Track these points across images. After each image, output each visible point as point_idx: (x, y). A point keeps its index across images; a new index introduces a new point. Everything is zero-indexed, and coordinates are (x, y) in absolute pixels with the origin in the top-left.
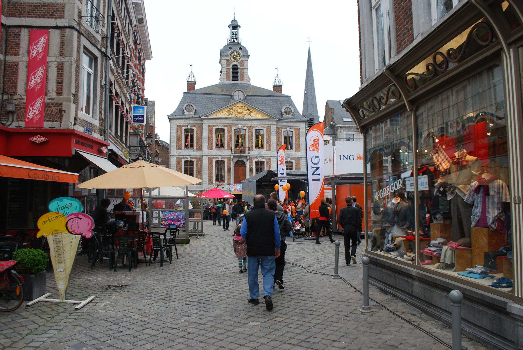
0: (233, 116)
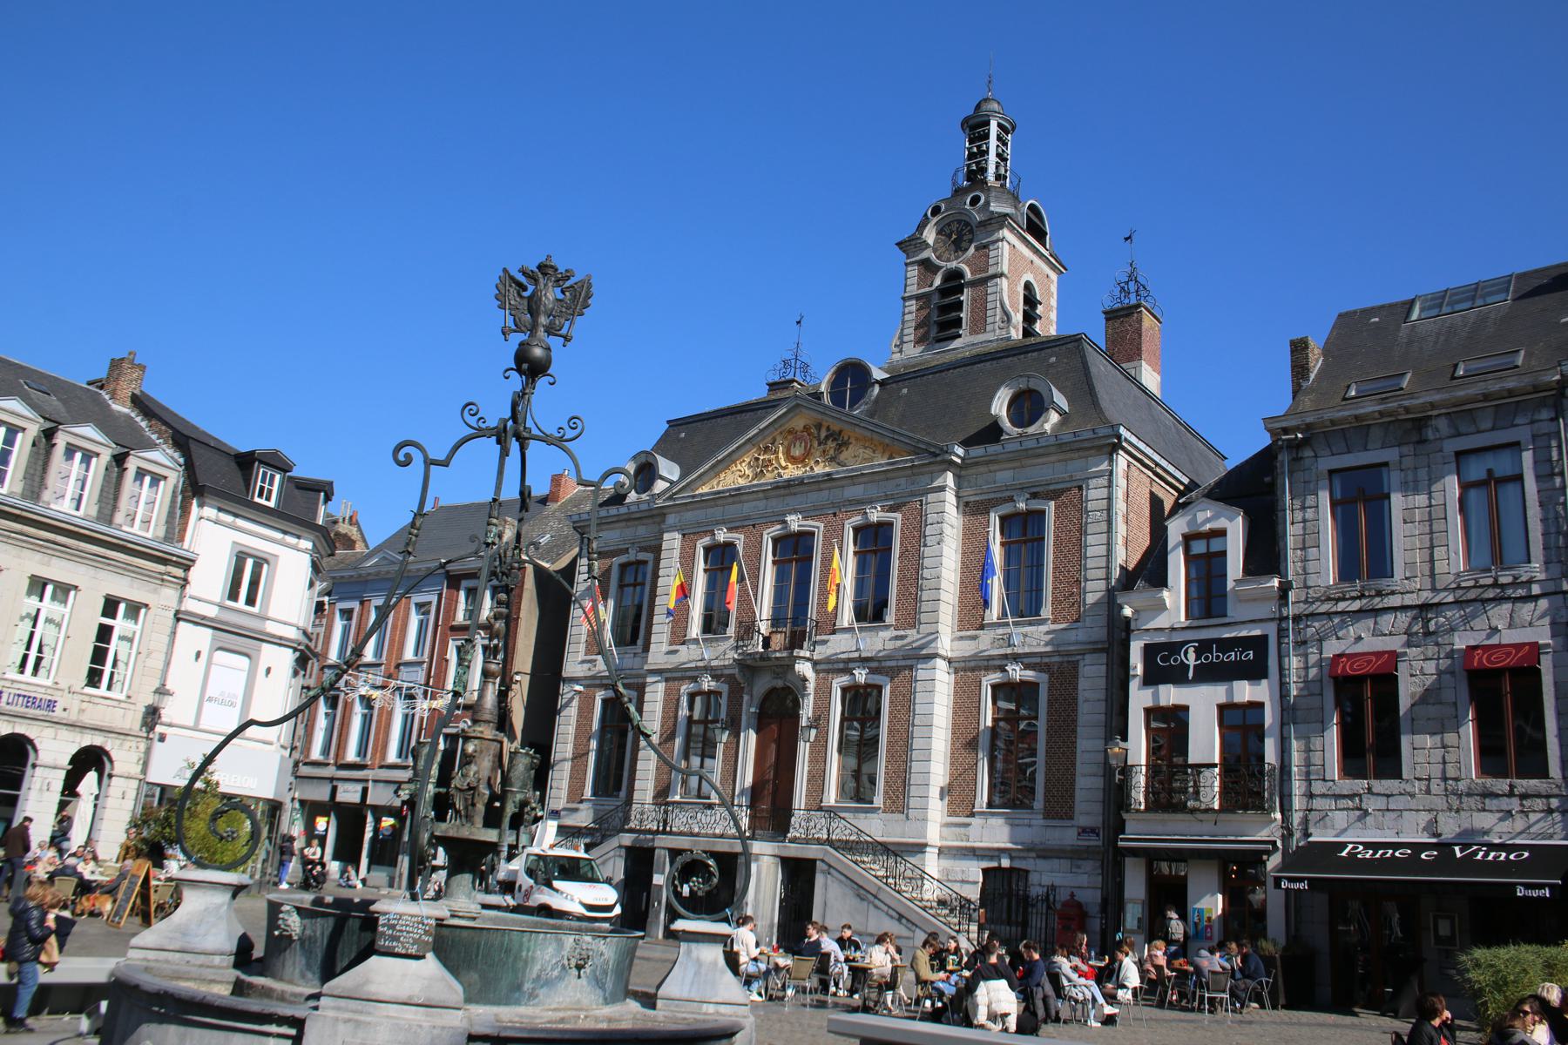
0: (769, 478)
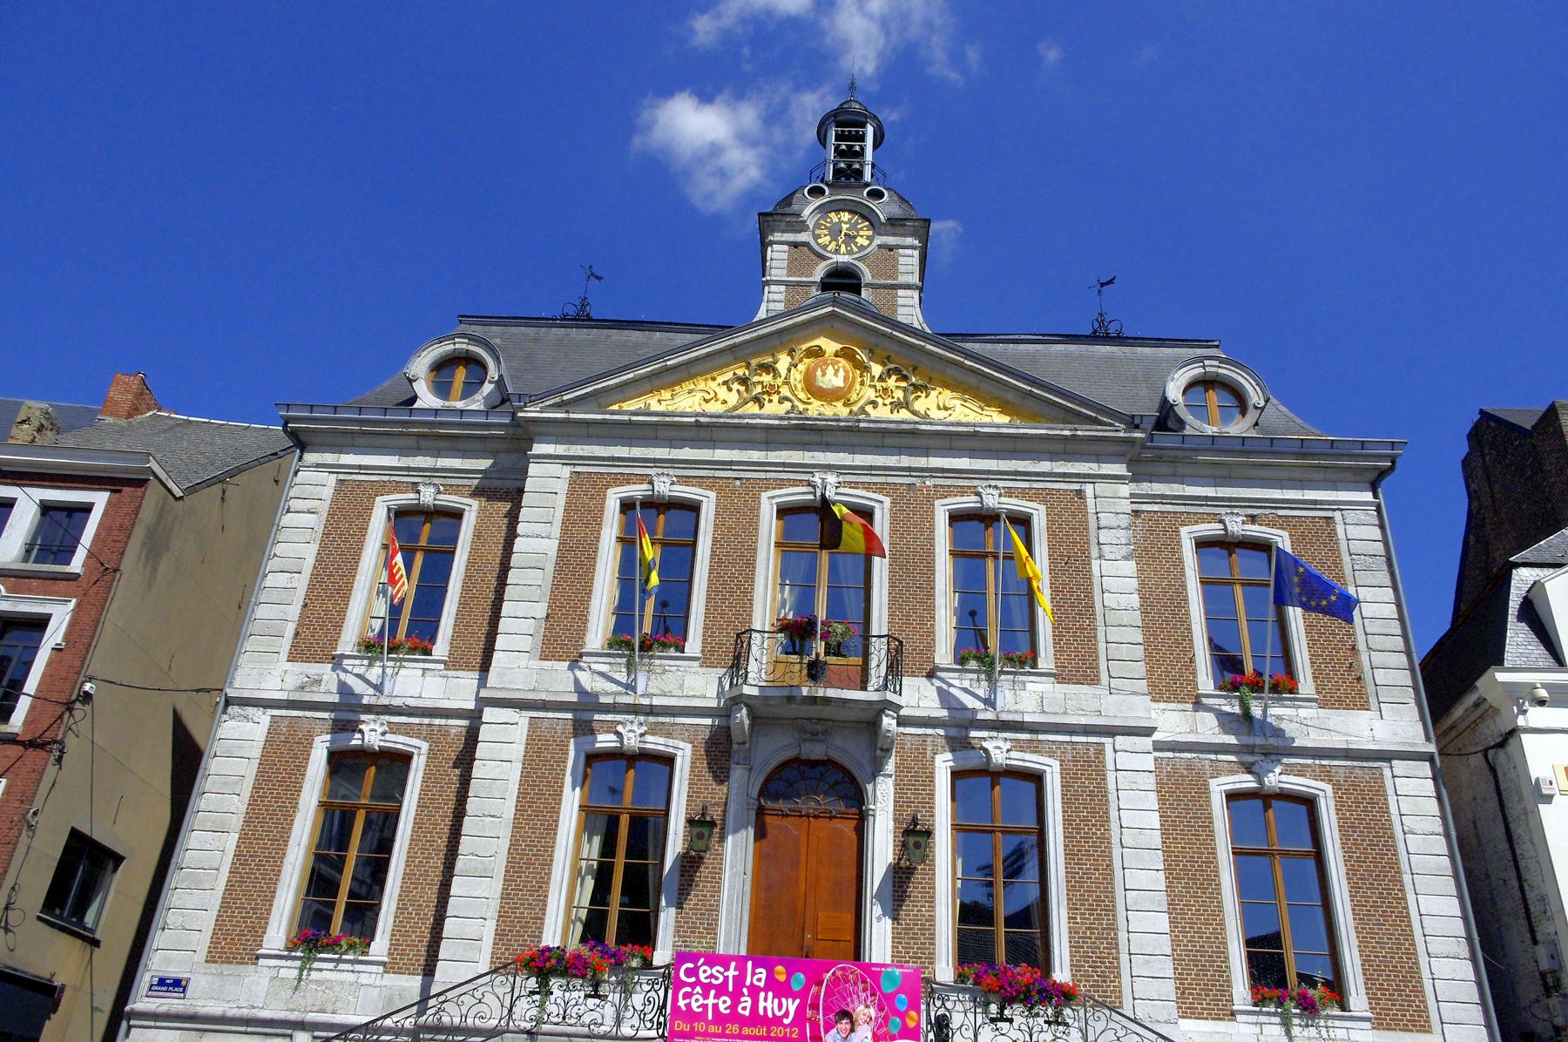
0: (774, 408)
